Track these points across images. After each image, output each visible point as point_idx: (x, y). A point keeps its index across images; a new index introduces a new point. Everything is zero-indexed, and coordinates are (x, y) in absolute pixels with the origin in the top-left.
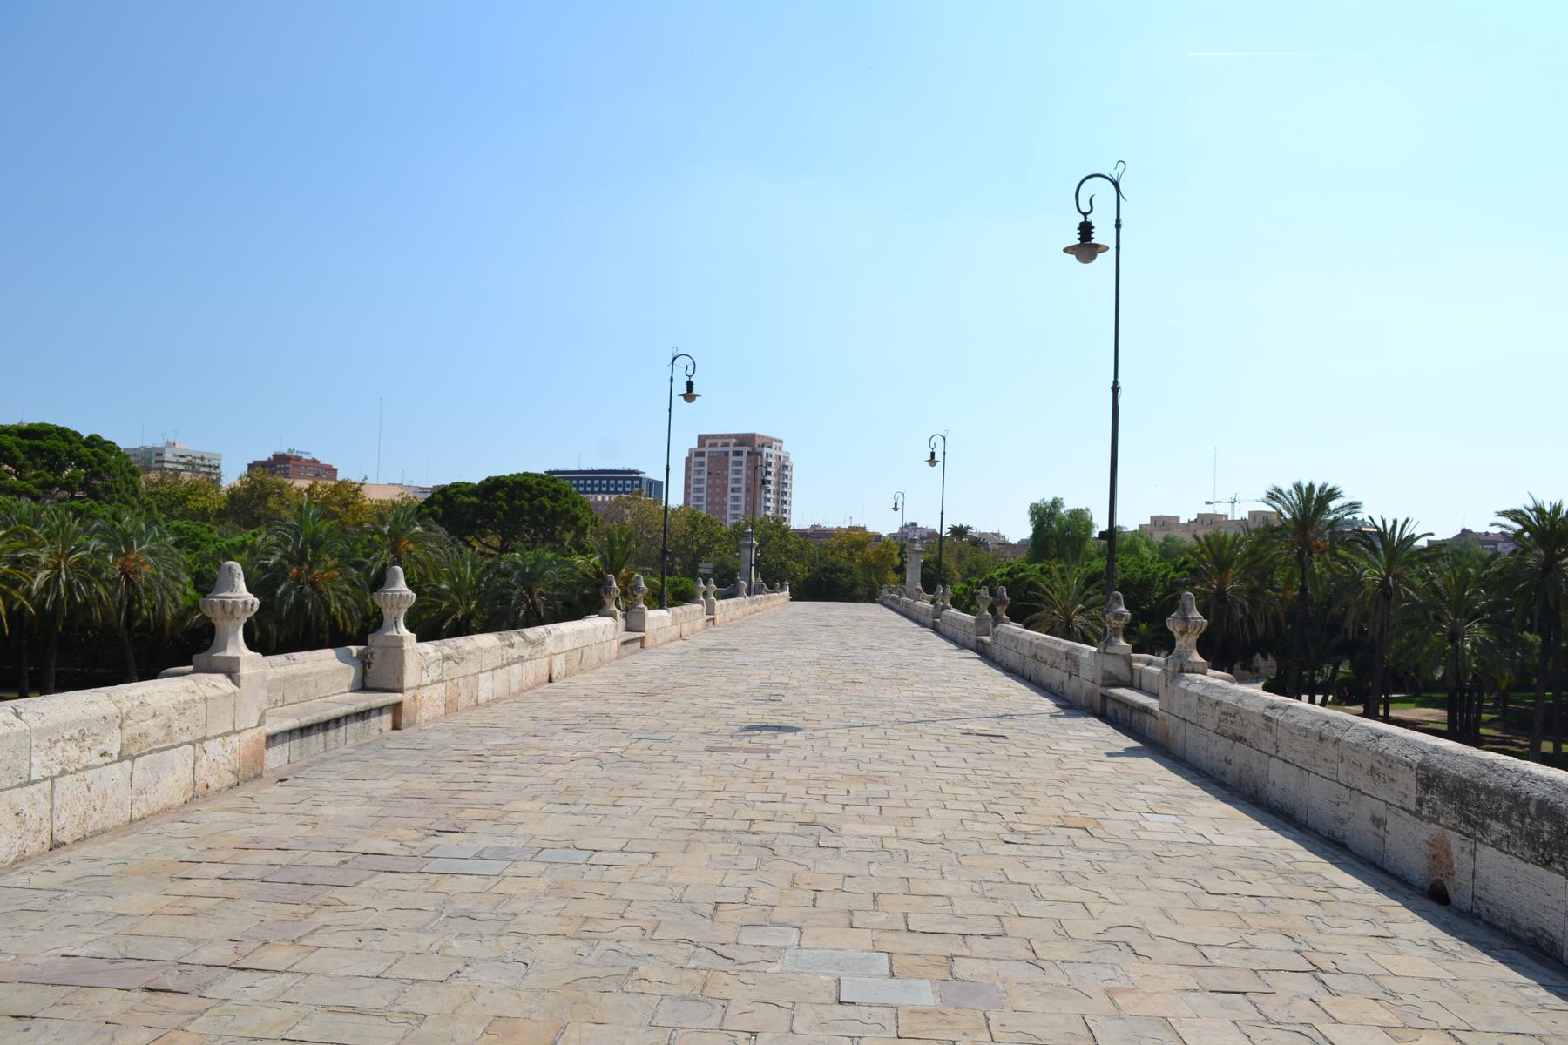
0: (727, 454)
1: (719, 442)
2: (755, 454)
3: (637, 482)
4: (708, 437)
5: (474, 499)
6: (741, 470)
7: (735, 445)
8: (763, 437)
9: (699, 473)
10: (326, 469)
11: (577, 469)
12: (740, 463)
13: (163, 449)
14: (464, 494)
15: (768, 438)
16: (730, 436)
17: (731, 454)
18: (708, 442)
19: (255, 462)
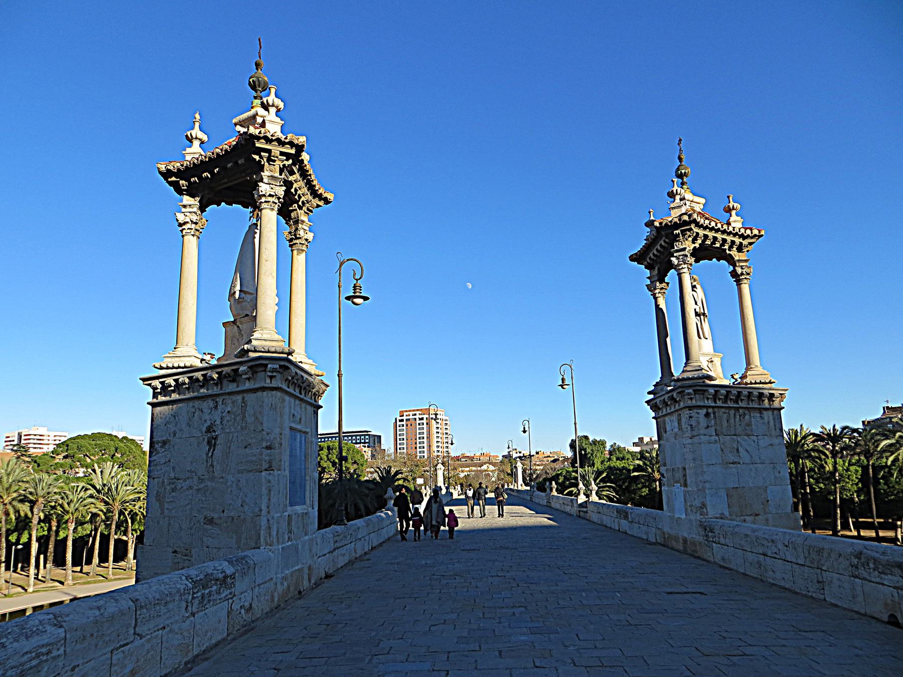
1: (411, 413)
3: (367, 437)
17: (418, 419)
18: (405, 414)
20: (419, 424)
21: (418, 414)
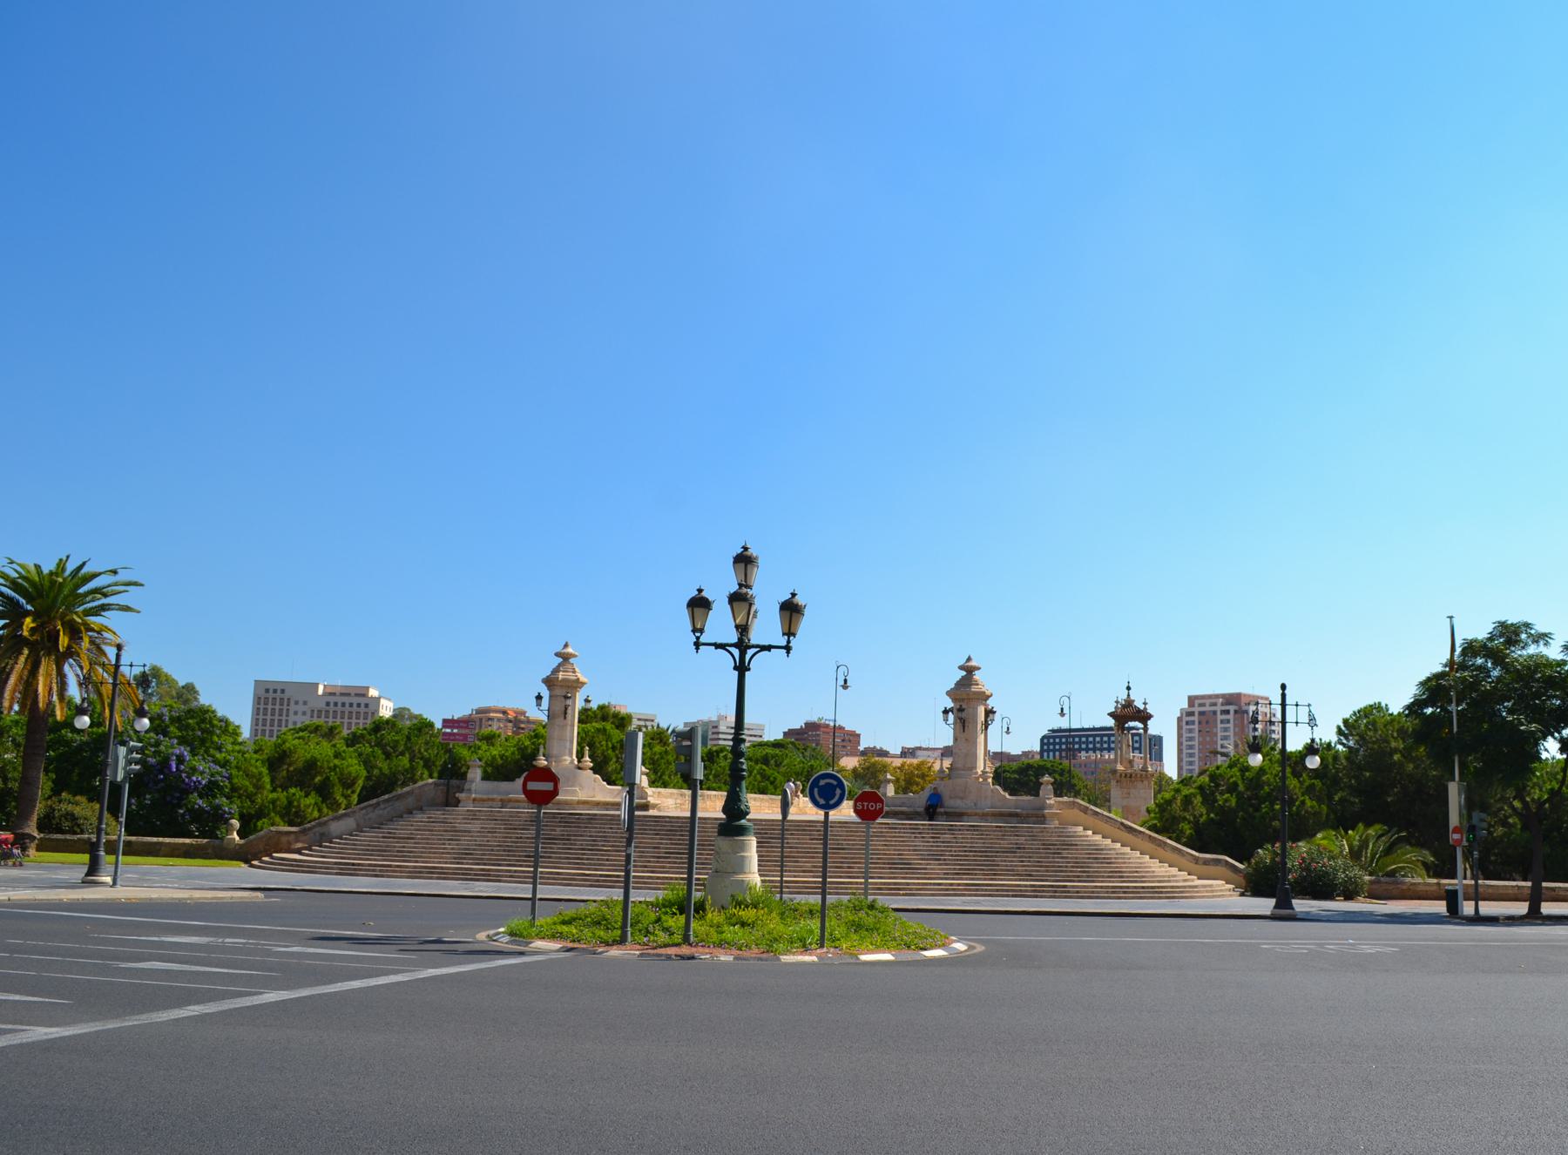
0: (1215, 713)
1: (1208, 702)
2: (1240, 712)
4: (1197, 697)
5: (1016, 776)
6: (1229, 728)
7: (1222, 705)
8: (1249, 696)
9: (1190, 731)
10: (851, 735)
11: (1079, 727)
12: (1228, 721)
13: (718, 721)
14: (1008, 771)
15: (1254, 696)
16: (1217, 696)
17: (1219, 713)
18: (1197, 702)
19: (789, 730)
20: (1222, 722)
21: (1219, 705)
